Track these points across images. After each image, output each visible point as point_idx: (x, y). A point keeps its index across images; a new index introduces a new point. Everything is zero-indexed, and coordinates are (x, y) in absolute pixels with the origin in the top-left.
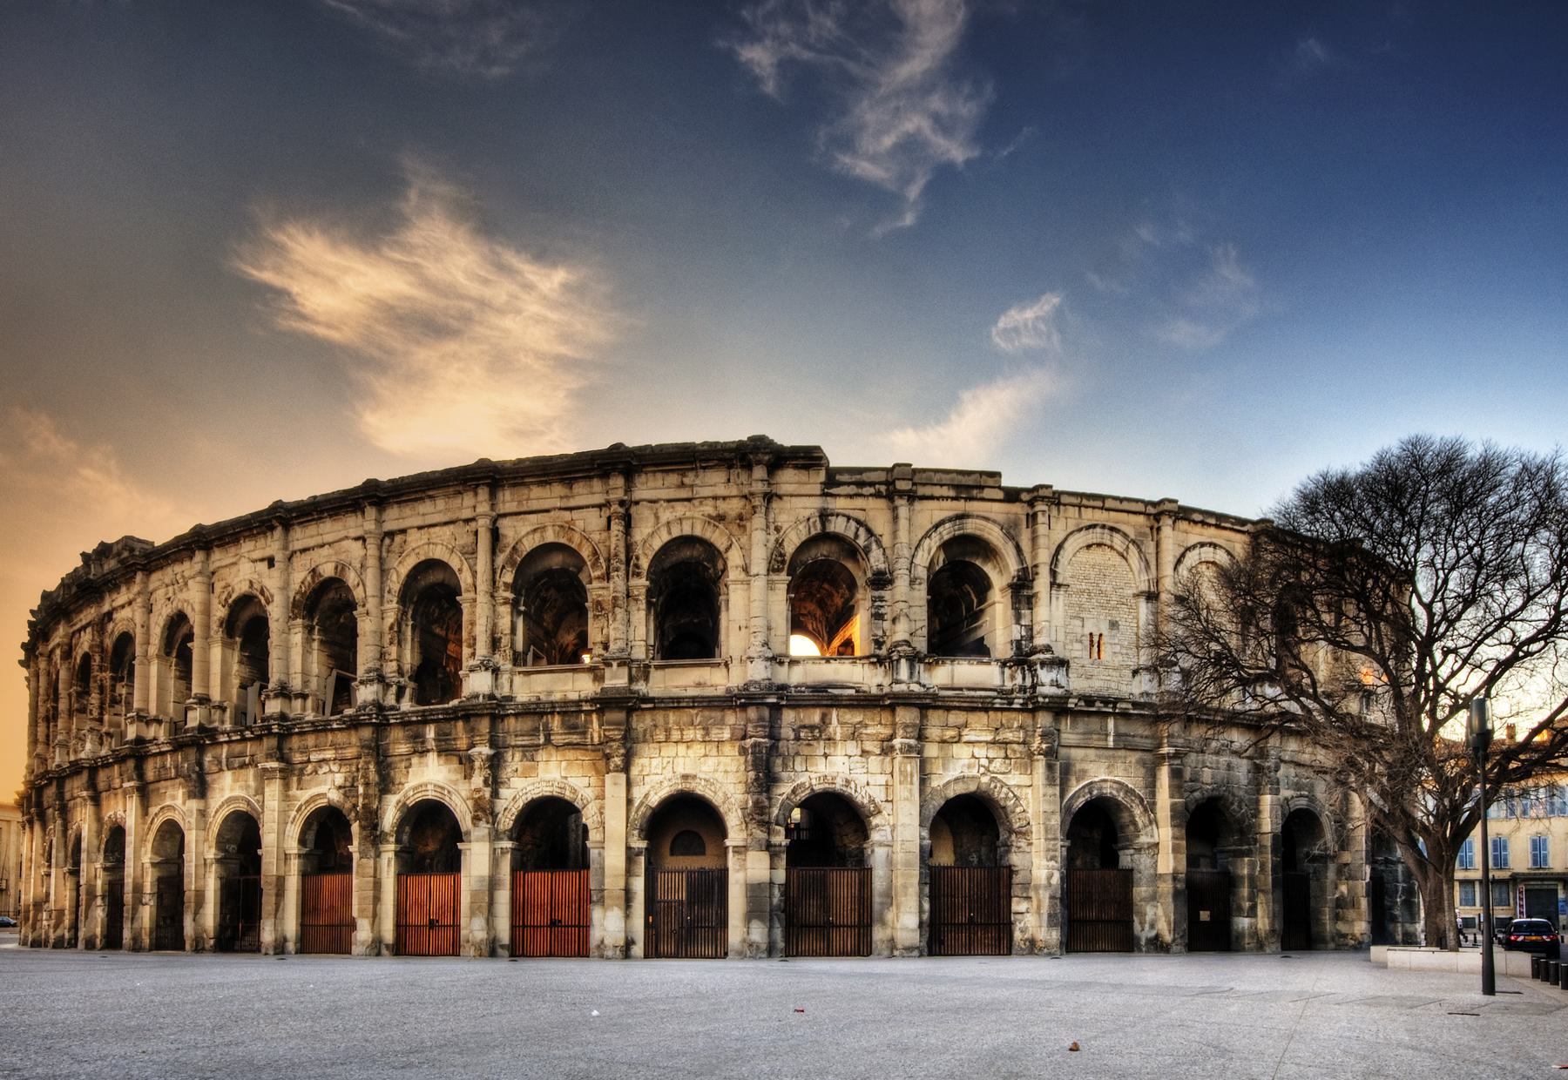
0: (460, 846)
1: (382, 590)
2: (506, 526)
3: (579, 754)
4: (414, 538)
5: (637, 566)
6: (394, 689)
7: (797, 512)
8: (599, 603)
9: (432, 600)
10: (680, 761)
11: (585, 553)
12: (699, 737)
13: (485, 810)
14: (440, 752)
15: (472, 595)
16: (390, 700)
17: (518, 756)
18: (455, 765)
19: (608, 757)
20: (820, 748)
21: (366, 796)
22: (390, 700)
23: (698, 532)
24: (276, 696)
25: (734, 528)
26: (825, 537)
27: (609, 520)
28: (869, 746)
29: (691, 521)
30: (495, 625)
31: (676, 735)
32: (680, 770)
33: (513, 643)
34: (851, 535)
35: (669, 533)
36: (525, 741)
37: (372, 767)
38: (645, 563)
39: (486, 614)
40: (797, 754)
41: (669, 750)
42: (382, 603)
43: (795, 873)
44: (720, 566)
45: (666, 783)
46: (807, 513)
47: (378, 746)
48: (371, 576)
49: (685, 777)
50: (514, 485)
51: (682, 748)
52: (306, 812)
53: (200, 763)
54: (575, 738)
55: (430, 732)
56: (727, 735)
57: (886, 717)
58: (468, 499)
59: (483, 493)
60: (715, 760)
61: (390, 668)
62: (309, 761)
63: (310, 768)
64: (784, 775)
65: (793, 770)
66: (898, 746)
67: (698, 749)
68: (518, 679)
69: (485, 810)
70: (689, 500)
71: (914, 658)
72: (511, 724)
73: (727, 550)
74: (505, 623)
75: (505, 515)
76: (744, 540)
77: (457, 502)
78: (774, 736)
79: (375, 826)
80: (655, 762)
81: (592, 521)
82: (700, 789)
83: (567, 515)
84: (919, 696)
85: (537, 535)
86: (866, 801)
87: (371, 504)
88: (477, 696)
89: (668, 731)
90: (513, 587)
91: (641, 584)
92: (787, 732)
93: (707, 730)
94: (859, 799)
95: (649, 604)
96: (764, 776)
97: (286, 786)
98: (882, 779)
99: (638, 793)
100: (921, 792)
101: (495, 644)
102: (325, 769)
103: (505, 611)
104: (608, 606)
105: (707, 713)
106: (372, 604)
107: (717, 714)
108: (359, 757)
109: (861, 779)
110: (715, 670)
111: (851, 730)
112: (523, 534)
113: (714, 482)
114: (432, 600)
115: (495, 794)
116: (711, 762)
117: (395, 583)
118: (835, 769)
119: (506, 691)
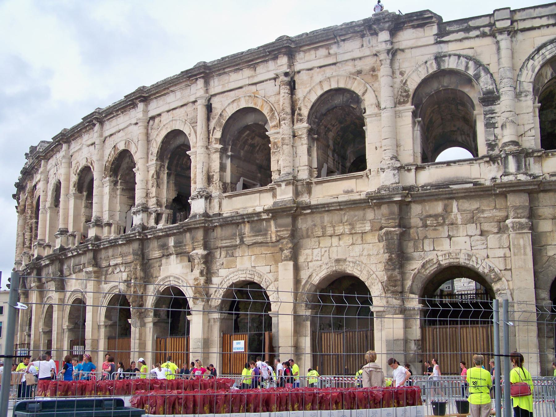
0: (189, 317)
3: (263, 250)
4: (165, 118)
5: (300, 115)
6: (153, 216)
7: (418, 56)
8: (275, 143)
9: (175, 154)
10: (334, 249)
12: (347, 231)
13: (204, 292)
17: (223, 254)
18: (186, 263)
19: (282, 250)
20: (444, 231)
21: (135, 286)
22: (152, 223)
23: (342, 85)
24: (93, 226)
25: (368, 78)
26: (440, 74)
28: (486, 227)
31: (330, 231)
32: (334, 256)
33: (221, 179)
34: (462, 68)
37: (139, 268)
38: (305, 112)
39: (204, 160)
40: (426, 237)
42: (147, 162)
43: (429, 330)
45: (324, 267)
48: (141, 145)
49: (338, 261)
50: (220, 75)
51: (335, 240)
52: (109, 297)
53: (61, 271)
54: (260, 239)
55: (171, 242)
56: (368, 228)
57: (500, 202)
59: (200, 83)
61: (152, 203)
62: (109, 266)
63: (110, 270)
64: (416, 254)
65: (423, 250)
66: (510, 225)
67: (347, 240)
68: (225, 202)
69: (204, 292)
72: (219, 232)
73: (364, 94)
74: (216, 165)
75: (215, 95)
76: (376, 85)
77: (187, 92)
79: (141, 305)
80: (316, 251)
82: (350, 270)
83: (253, 88)
85: (235, 104)
86: (486, 271)
87: (140, 101)
89: (324, 228)
90: (222, 141)
91: (303, 127)
92: (415, 221)
93: (352, 225)
94: (480, 270)
96: (398, 258)
97: (99, 282)
98: (501, 253)
99: (304, 275)
100: (535, 263)
101: (209, 179)
102: (118, 270)
104: (280, 145)
105: (352, 213)
107: (360, 213)
111: (469, 216)
112: (226, 107)
114: (175, 154)
115: (208, 281)
116: (357, 249)
117: (155, 148)
119: (216, 211)
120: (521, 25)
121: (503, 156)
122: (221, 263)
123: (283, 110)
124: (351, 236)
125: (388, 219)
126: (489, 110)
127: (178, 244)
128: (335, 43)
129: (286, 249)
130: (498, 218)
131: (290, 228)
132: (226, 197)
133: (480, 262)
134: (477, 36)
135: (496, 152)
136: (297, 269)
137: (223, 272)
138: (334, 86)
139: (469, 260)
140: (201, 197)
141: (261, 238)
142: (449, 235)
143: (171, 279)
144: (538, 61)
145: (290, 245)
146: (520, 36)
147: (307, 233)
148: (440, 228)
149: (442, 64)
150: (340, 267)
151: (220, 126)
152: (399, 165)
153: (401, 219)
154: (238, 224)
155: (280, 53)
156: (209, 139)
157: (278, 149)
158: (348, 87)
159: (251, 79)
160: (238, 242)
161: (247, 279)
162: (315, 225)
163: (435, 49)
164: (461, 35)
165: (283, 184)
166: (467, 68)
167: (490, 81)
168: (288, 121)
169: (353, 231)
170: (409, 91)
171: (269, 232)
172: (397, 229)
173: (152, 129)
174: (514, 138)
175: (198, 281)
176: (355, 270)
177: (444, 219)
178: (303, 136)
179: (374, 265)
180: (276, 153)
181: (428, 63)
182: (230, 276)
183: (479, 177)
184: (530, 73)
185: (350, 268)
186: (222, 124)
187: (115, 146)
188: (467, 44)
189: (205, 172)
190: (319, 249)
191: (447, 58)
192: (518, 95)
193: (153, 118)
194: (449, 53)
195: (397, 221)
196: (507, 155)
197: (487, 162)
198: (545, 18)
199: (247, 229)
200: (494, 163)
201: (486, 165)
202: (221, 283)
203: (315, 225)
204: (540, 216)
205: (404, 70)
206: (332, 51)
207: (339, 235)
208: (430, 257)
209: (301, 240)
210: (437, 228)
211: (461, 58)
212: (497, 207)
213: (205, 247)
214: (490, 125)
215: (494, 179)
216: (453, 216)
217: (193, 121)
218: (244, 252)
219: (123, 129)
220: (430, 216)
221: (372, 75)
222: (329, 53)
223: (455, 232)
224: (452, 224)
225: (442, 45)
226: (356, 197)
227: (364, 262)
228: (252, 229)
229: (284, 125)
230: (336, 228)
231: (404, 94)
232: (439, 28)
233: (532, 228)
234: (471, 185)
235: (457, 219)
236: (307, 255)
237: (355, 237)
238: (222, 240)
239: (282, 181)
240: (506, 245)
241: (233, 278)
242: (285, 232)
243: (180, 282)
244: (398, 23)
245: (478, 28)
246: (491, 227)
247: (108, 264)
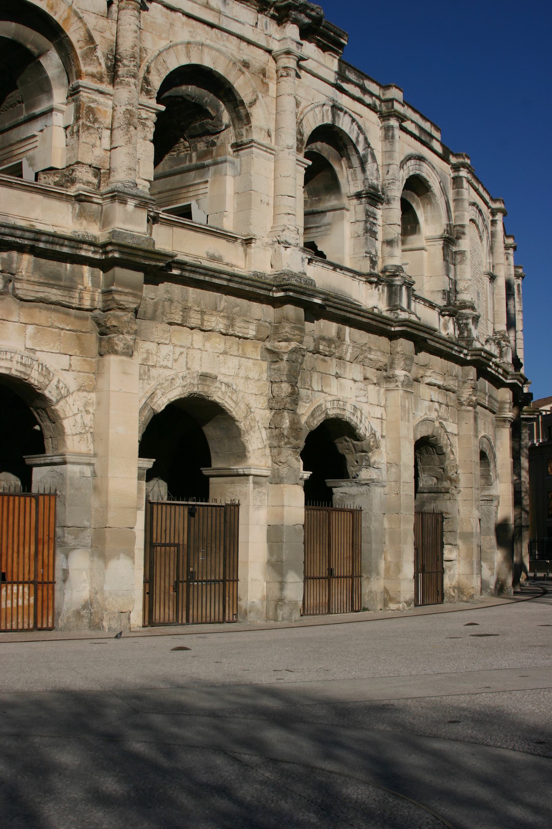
23: (220, 70)
32: (198, 367)
34: (353, 137)
38: (157, 82)
41: (184, 336)
45: (179, 382)
49: (204, 377)
54: (54, 294)
60: (236, 360)
67: (218, 344)
80: (165, 350)
121: (398, 283)
129: (128, 333)
134: (368, 106)
138: (207, 62)
139: (354, 415)
141: (59, 292)
149: (337, 118)
150: (206, 389)
157: (96, 126)
164: (356, 92)
169: (231, 332)
176: (227, 399)
179: (254, 397)
180: (92, 131)
190: (171, 347)
191: (342, 114)
198: (413, 125)
203: (171, 301)
210: (326, 358)
227: (241, 387)
228: (37, 268)
230: (206, 317)
235: (346, 352)
236: (148, 352)
239: (134, 197)
242: (130, 299)
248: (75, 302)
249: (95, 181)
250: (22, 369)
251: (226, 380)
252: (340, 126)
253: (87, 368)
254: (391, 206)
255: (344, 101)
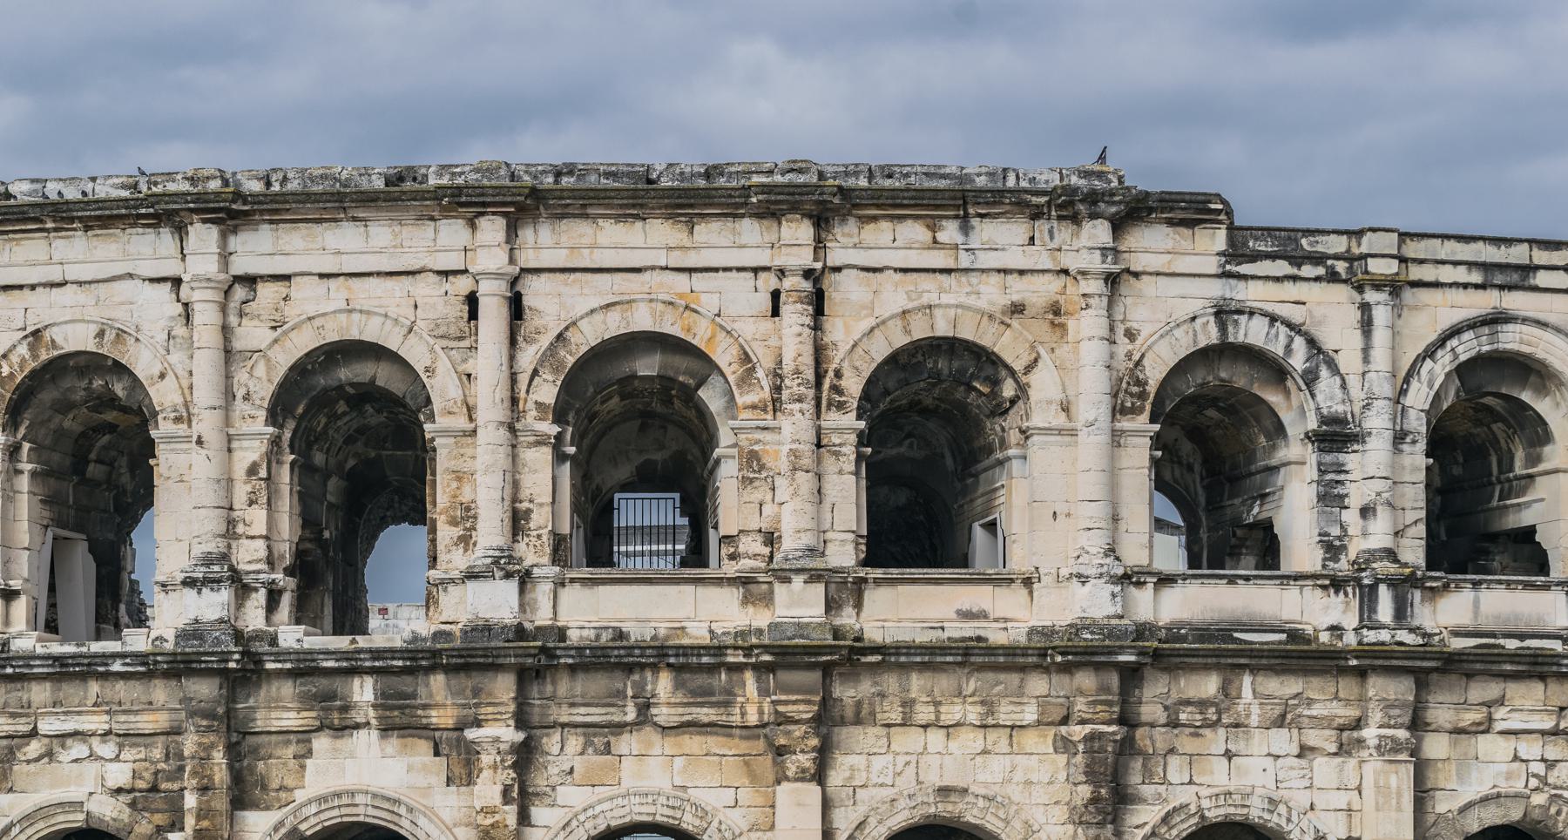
1: (229, 395)
2: (536, 293)
3: (713, 743)
4: (308, 297)
5: (836, 389)
6: (260, 597)
10: (934, 761)
11: (724, 356)
14: (386, 730)
15: (462, 422)
16: (254, 617)
17: (574, 742)
19: (780, 752)
20: (1216, 740)
23: (967, 333)
25: (1041, 329)
27: (776, 295)
28: (1313, 737)
29: (959, 310)
30: (516, 485)
31: (924, 713)
32: (934, 779)
34: (1279, 350)
35: (908, 332)
36: (595, 715)
37: (219, 757)
38: (853, 386)
40: (1172, 751)
42: (227, 422)
44: (1008, 390)
45: (902, 803)
46: (1195, 306)
47: (229, 713)
48: (206, 365)
49: (944, 791)
50: (562, 216)
51: (936, 738)
54: (706, 714)
55: (363, 691)
56: (1030, 714)
57: (1347, 687)
58: (452, 232)
59: (492, 229)
61: (249, 555)
62: (34, 733)
63: (34, 748)
64: (1147, 790)
65: (1165, 781)
66: (1373, 742)
67: (971, 740)
70: (948, 271)
71: (1403, 585)
73: (1029, 369)
76: (1063, 351)
78: (1127, 720)
80: (878, 763)
81: (742, 300)
84: (1411, 654)
88: (487, 629)
89: (908, 704)
91: (845, 424)
92: (1151, 711)
93: (989, 705)
95: (860, 457)
98: (1341, 799)
101: (518, 522)
102: (78, 749)
103: (545, 454)
106: (207, 424)
107: (1014, 678)
108: (175, 731)
109: (1301, 799)
110: (1002, 592)
111: (1278, 711)
113: (1002, 238)
115: (524, 818)
117: (261, 382)
118: (1247, 781)
119: (543, 617)
120: (1416, 273)
121: (1366, 581)
122: (567, 767)
123: (797, 372)
124: (980, 734)
125: (1094, 703)
126: (1332, 464)
127: (385, 701)
128: (956, 217)
129: (802, 751)
130: (1341, 721)
131: (818, 698)
132: (572, 580)
133: (1295, 818)
134: (1317, 279)
135: (1343, 566)
136: (827, 805)
137: (572, 796)
138: (942, 329)
139: (1272, 812)
140: (508, 576)
141: (712, 711)
142: (1227, 751)
143: (359, 799)
144: (1442, 365)
145: (814, 742)
146: (1408, 295)
147: (858, 713)
148: (1207, 732)
149: (1231, 329)
150: (950, 807)
151: (556, 371)
152: (1120, 571)
153: (1124, 702)
154: (629, 669)
155: (794, 208)
156: (514, 401)
157: (764, 474)
158: (986, 342)
159: (677, 253)
160: (631, 714)
161: (659, 818)
162: (882, 695)
163: (1217, 289)
164: (1282, 267)
165: (798, 581)
166: (1288, 349)
167: (1339, 393)
168: (808, 406)
169: (990, 721)
170: (1146, 383)
171: (740, 699)
172: (1113, 728)
173: (241, 315)
174: (1387, 542)
175: (497, 817)
177: (1219, 713)
178: (844, 450)
179: (1042, 809)
180: (757, 483)
181: (1198, 321)
182: (598, 809)
183: (1298, 618)
184: (1425, 389)
185: (975, 811)
186: (562, 363)
187: (36, 333)
188: (1292, 291)
189: (507, 503)
190: (890, 757)
191: (1243, 319)
192: (1399, 437)
193: (251, 281)
194: (1254, 304)
195: (1116, 709)
196: (1378, 581)
197: (1324, 587)
199: (663, 685)
200: (1337, 592)
201: (1319, 592)
202: (568, 824)
203: (882, 695)
204: (1428, 724)
205: (1135, 325)
206: (942, 237)
207: (947, 727)
208: (1183, 800)
209: (836, 729)
210: (1201, 731)
211: (1278, 324)
212: (1341, 695)
213: (521, 721)
214: (1330, 497)
215: (1335, 629)
216: (1240, 708)
217: (441, 331)
218: (650, 744)
219: (80, 283)
220: (1188, 703)
221: (1052, 323)
222: (935, 241)
223: (1242, 744)
224: (1237, 726)
225: (1233, 282)
226: (997, 637)
227: (1016, 798)
228: (678, 685)
229: (799, 415)
230: (943, 709)
231: (1135, 389)
232: (1231, 241)
233: (1415, 752)
234: (1283, 636)
235: (1248, 716)
236: (852, 769)
237: (992, 735)
238: (572, 705)
239: (799, 571)
240: (1354, 783)
241: (609, 815)
242: (802, 707)
243: (402, 810)
244: (1135, 210)
245: (1318, 259)
246: (1323, 739)
247: (23, 727)
248: (736, 719)
249: (767, 551)
250: (670, 812)
251: (982, 791)
252: (1241, 339)
253: (760, 801)
254: (1368, 447)
255: (1251, 293)
